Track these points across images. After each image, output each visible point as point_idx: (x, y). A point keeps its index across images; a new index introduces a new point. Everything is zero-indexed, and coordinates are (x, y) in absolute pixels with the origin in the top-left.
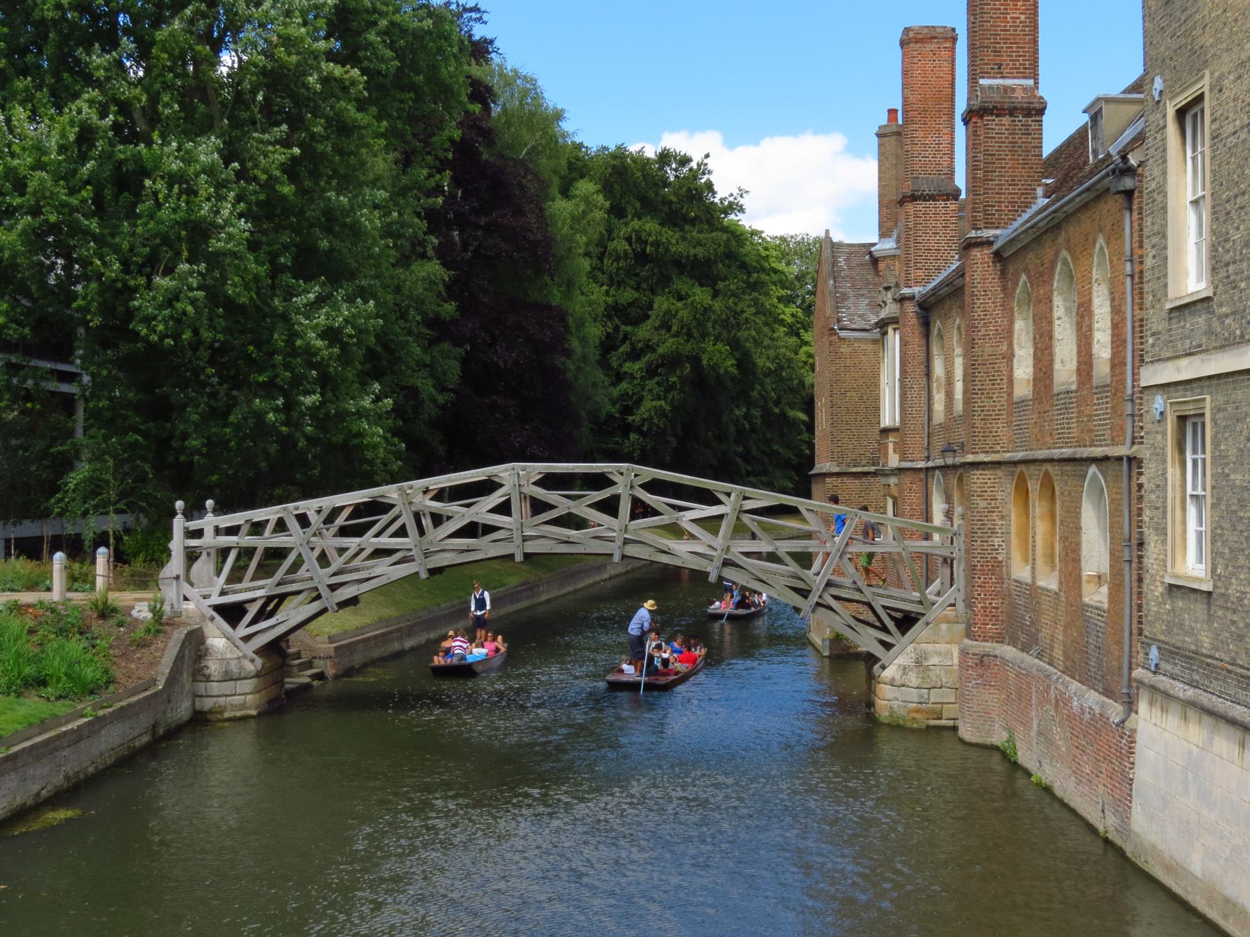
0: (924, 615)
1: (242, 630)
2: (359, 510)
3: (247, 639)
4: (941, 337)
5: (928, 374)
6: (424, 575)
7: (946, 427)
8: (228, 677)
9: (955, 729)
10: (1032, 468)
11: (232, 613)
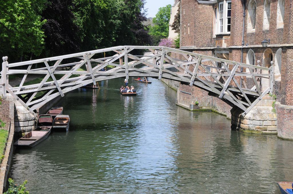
0: (259, 97)
1: (29, 103)
3: (30, 106)
6: (95, 84)
9: (276, 134)
11: (25, 98)
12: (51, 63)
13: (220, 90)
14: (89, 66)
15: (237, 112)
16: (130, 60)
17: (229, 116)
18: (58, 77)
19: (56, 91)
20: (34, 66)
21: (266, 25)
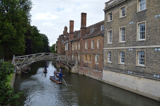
2: (29, 56)
3: (20, 67)
4: (73, 44)
5: (72, 46)
7: (74, 51)
8: (19, 70)
10: (88, 54)
12: (26, 57)
13: (66, 63)
14: (35, 57)
15: (70, 68)
16: (45, 56)
17: (68, 69)
18: (27, 60)
19: (26, 63)
20: (21, 58)
21: (76, 49)
